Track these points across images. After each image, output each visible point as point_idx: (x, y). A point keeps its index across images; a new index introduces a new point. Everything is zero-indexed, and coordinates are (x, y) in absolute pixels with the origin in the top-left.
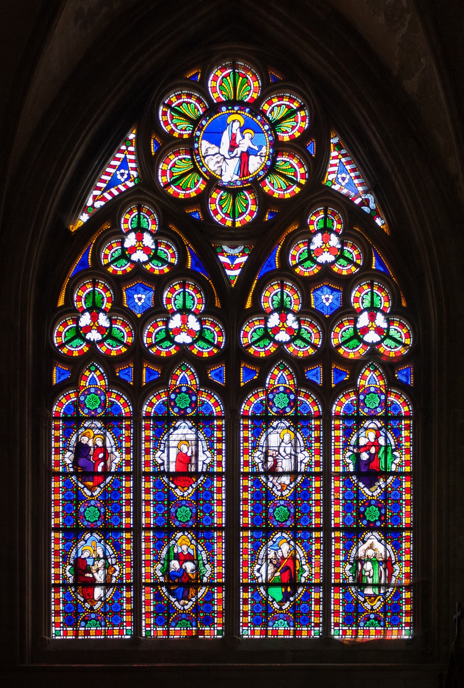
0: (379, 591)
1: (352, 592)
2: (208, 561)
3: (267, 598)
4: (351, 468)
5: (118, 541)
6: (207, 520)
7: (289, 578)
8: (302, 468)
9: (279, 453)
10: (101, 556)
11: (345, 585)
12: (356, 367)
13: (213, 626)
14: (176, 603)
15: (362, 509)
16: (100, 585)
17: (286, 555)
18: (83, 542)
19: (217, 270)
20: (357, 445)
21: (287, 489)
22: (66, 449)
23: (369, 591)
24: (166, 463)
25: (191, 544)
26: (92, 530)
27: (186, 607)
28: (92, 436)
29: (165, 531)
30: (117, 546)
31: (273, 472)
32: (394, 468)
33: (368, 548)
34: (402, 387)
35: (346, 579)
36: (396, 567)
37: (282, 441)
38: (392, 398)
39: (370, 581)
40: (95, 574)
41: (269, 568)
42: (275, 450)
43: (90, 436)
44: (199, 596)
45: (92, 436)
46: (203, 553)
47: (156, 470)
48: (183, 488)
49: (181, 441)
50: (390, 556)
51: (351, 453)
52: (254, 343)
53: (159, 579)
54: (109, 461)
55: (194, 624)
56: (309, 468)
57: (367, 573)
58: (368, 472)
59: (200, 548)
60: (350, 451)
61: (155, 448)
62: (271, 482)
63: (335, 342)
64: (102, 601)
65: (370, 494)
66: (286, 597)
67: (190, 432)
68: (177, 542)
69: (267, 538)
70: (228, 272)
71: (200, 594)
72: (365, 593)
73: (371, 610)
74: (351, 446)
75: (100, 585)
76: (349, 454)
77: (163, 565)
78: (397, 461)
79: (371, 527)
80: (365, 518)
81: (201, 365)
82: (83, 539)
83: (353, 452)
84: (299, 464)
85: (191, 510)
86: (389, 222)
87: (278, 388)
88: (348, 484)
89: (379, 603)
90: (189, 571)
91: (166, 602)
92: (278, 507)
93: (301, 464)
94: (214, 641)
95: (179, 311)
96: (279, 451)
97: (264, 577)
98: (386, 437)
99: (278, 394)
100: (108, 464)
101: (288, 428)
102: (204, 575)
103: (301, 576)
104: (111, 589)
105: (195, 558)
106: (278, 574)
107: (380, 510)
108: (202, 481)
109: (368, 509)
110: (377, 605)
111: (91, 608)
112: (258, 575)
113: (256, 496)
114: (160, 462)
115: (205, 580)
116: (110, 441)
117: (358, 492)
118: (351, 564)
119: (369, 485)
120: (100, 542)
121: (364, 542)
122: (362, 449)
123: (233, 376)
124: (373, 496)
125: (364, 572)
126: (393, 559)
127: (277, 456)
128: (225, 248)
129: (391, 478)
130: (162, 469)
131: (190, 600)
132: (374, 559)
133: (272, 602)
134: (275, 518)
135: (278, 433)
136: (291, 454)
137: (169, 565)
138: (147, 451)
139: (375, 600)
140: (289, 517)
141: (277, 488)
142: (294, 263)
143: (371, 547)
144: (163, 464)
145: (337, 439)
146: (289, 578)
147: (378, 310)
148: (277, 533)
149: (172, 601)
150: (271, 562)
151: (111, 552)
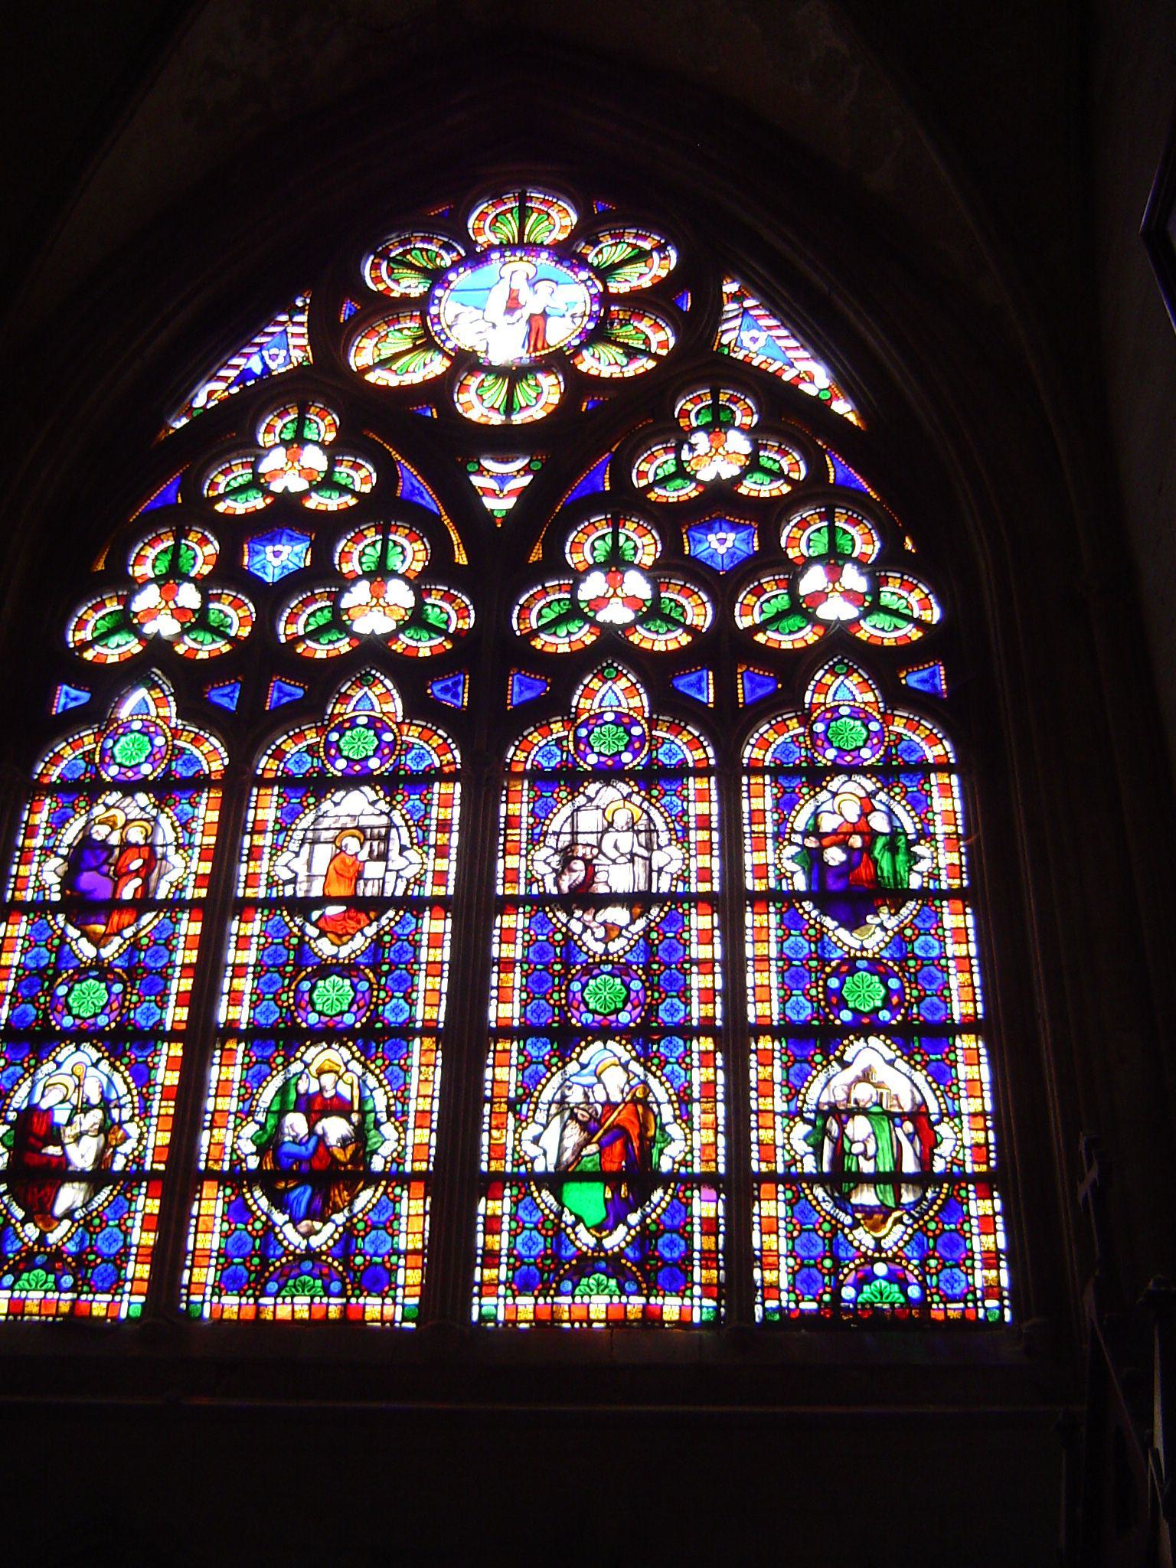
0: (898, 1196)
1: (816, 1198)
2: (390, 1114)
3: (559, 1215)
4: (800, 883)
5: (146, 1062)
6: (397, 1010)
7: (625, 1158)
8: (664, 885)
9: (601, 852)
10: (95, 1099)
11: (791, 1179)
12: (795, 669)
13: (391, 1293)
14: (289, 1229)
15: (834, 983)
16: (79, 1176)
17: (616, 1097)
18: (51, 1066)
19: (465, 504)
20: (814, 831)
21: (620, 935)
22: (48, 851)
23: (866, 1196)
24: (301, 878)
25: (347, 1070)
26: (79, 1036)
27: (315, 1241)
28: (119, 819)
29: (278, 1038)
30: (142, 1076)
31: (584, 898)
32: (915, 882)
33: (858, 1080)
34: (921, 704)
35: (794, 1161)
36: (944, 1130)
37: (611, 824)
38: (898, 727)
39: (867, 1167)
40: (71, 1149)
41: (567, 1132)
42: (588, 845)
43: (115, 823)
44: (355, 1210)
45: (121, 822)
46: (379, 1094)
47: (274, 895)
48: (340, 936)
49: (343, 829)
50: (924, 1102)
51: (795, 849)
52: (543, 628)
53: (245, 1160)
54: (155, 875)
55: (335, 1286)
56: (680, 884)
57: (857, 1148)
58: (850, 891)
59: (372, 1081)
60: (791, 843)
61: (277, 849)
62: (579, 919)
63: (743, 623)
64: (74, 1221)
65: (857, 945)
66: (616, 1214)
67: (370, 809)
68: (307, 1066)
69: (564, 1058)
70: (489, 503)
71: (359, 1204)
72: (854, 1201)
73: (874, 1251)
74: (796, 832)
75: (79, 1176)
76: (792, 850)
77: (263, 1126)
78: (924, 866)
79: (865, 1026)
80: (843, 1004)
81: (410, 675)
82: (54, 1060)
83: (803, 846)
84: (655, 875)
85: (353, 986)
86: (861, 409)
87: (600, 715)
88: (792, 921)
89: (900, 1228)
90: (332, 1140)
91: (258, 1225)
92: (595, 977)
93: (659, 875)
94: (388, 1331)
95: (367, 575)
96: (599, 847)
97: (552, 1159)
98: (890, 813)
99: (601, 726)
100: (152, 884)
101: (626, 798)
102: (375, 1152)
103: (661, 1152)
104: (106, 1191)
105: (356, 1107)
106: (593, 1148)
107: (884, 982)
108: (391, 920)
109: (848, 979)
110: (894, 1235)
111: (42, 1240)
112: (531, 1150)
113: (535, 952)
114: (286, 875)
115: (377, 1164)
116: (166, 833)
117: (820, 937)
118: (806, 1121)
119: (853, 922)
120: (95, 1065)
121: (844, 1065)
122: (825, 842)
123: (488, 691)
124: (863, 949)
125: (847, 1145)
126: (933, 1107)
127: (596, 857)
128: (487, 463)
129: (911, 905)
130: (289, 891)
131: (325, 1221)
132: (877, 1109)
133: (573, 1226)
134: (587, 1004)
135: (598, 807)
136: (633, 855)
137: (279, 1127)
138: (255, 854)
139: (884, 1221)
140: (625, 1002)
141: (593, 933)
142: (643, 483)
143: (866, 1077)
144: (294, 881)
145: (757, 816)
146: (625, 1158)
147: (848, 558)
148: (592, 1042)
149: (275, 1225)
150: (573, 1116)
151: (122, 1089)
